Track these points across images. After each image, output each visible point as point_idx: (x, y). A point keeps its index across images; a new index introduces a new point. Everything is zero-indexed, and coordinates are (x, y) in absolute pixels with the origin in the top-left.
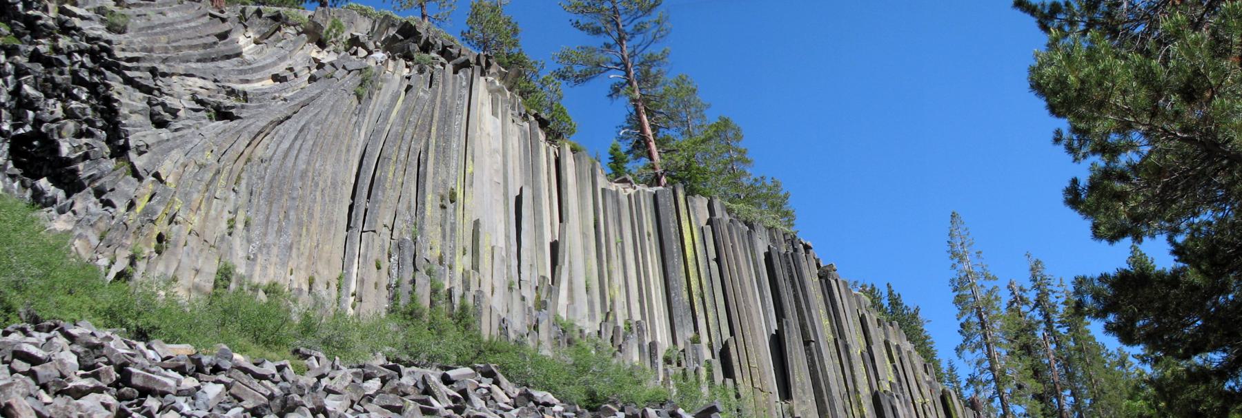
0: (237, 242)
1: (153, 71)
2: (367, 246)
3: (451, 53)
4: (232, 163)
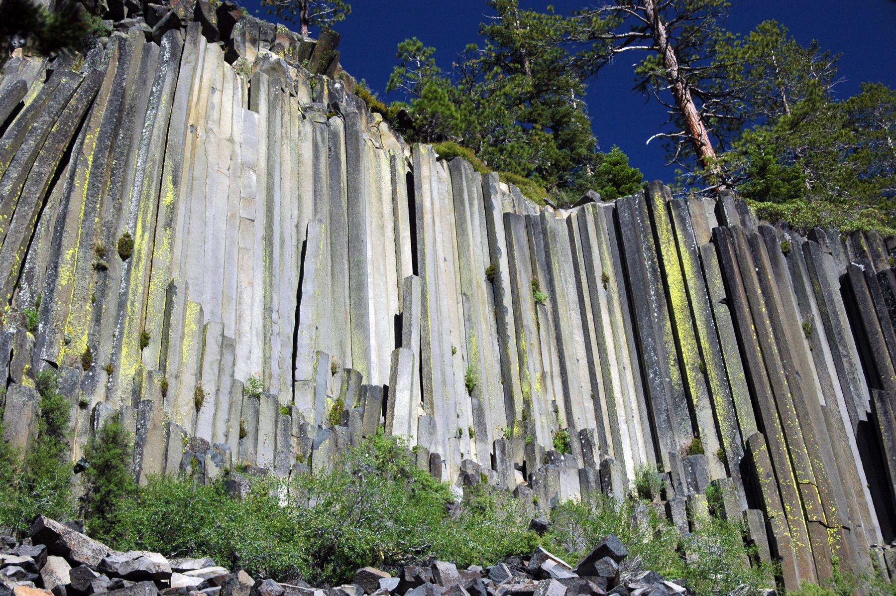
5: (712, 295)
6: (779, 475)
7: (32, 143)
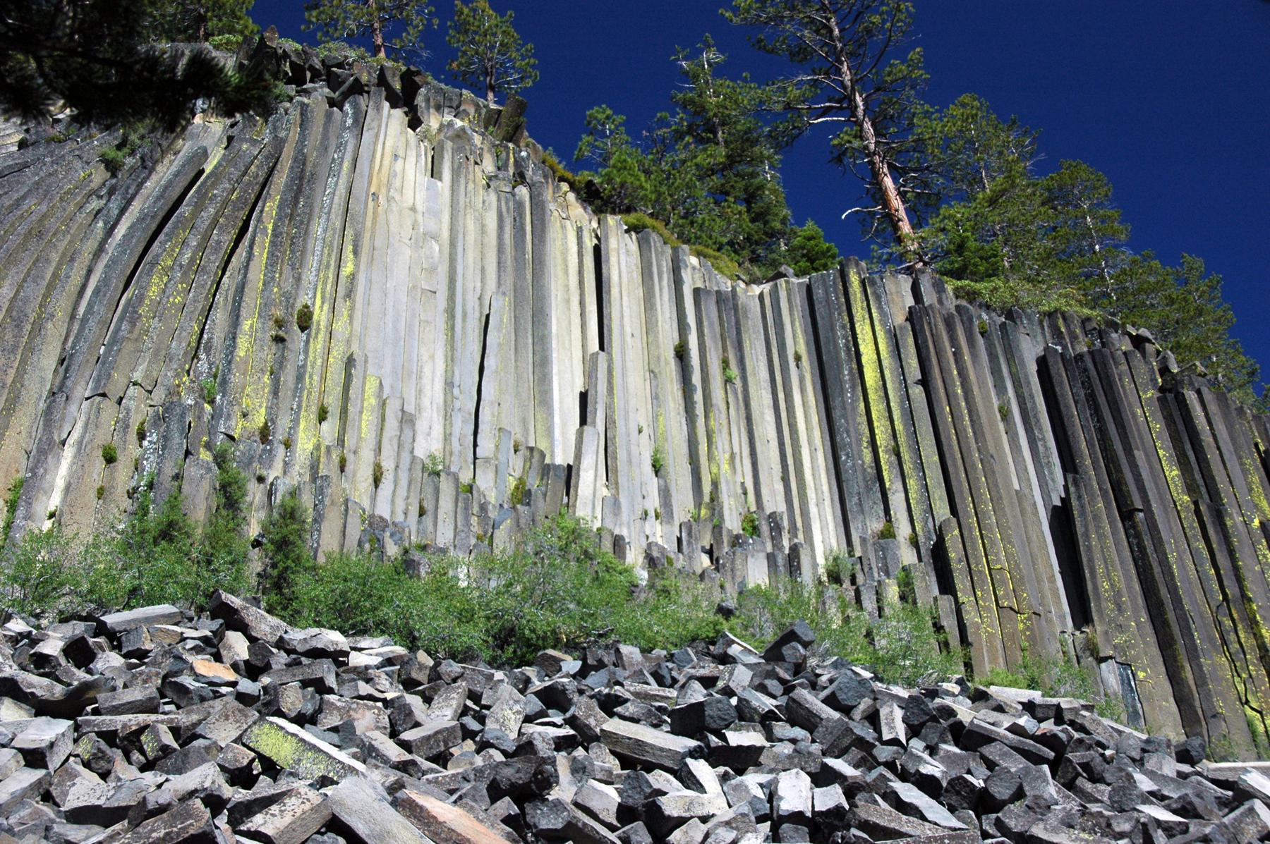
3: (338, 76)
5: (907, 375)
6: (971, 561)
7: (212, 210)
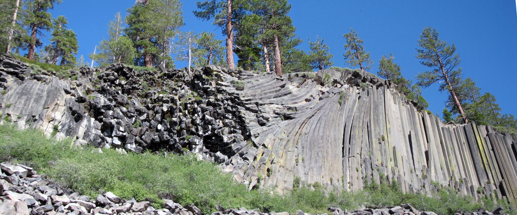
0: (300, 167)
1: (257, 104)
2: (352, 163)
3: (374, 81)
4: (294, 136)
